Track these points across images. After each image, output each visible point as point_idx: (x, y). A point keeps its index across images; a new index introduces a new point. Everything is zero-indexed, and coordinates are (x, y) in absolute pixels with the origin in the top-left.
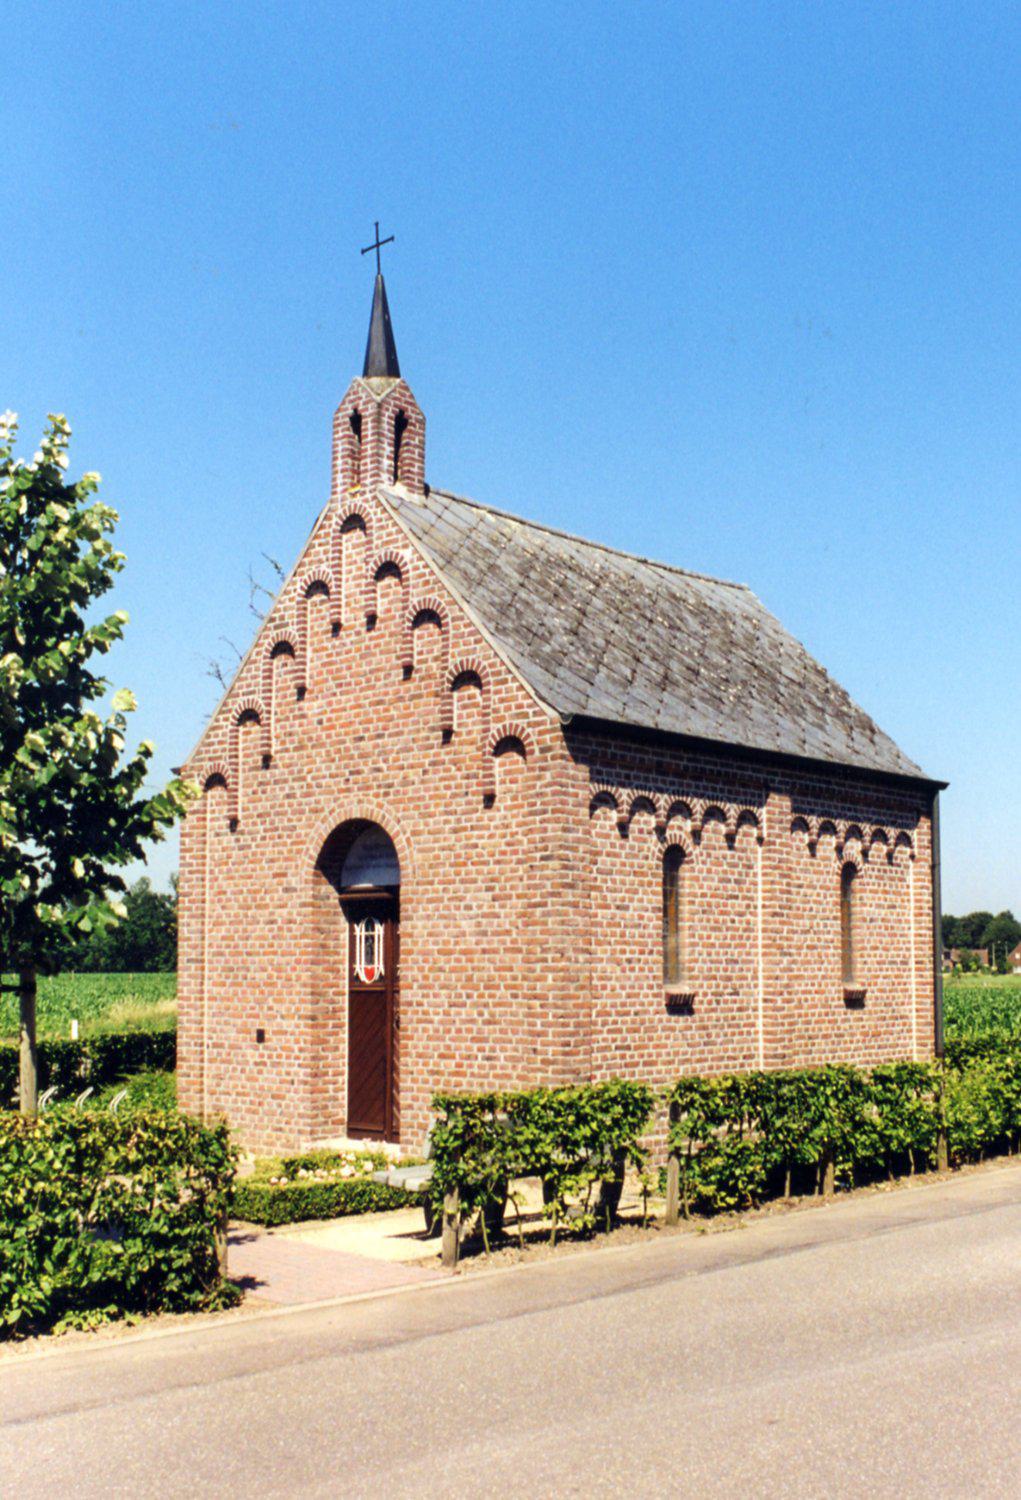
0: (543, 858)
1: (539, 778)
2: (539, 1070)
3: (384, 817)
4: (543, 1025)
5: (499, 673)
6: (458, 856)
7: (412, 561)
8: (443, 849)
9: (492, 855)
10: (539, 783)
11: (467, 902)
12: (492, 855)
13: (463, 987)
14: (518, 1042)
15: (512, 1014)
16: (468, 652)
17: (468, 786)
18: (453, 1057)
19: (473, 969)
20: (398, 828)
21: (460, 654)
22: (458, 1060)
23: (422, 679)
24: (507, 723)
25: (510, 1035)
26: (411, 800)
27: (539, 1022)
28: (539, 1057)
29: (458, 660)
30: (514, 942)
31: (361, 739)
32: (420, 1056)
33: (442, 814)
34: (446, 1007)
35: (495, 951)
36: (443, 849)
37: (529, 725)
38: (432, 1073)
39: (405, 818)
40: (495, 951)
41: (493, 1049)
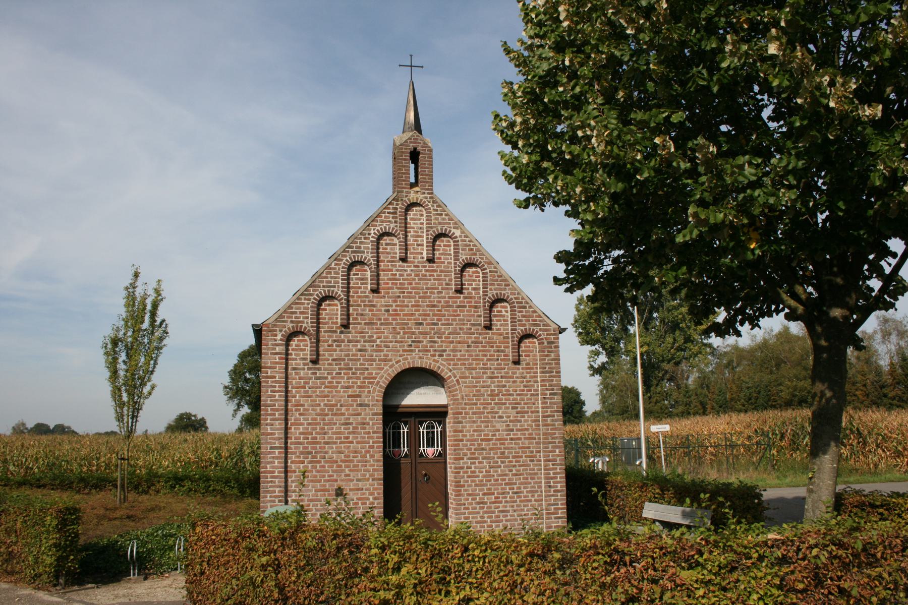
0: (551, 394)
1: (547, 356)
2: (553, 495)
3: (439, 367)
4: (554, 474)
5: (521, 303)
6: (493, 391)
7: (460, 236)
8: (483, 387)
9: (516, 391)
10: (547, 358)
11: (500, 414)
12: (516, 391)
13: (498, 458)
14: (534, 483)
15: (530, 470)
16: (501, 289)
17: (498, 356)
18: (493, 494)
19: (505, 448)
20: (450, 374)
21: (495, 290)
22: (496, 495)
23: (465, 298)
24: (528, 327)
25: (529, 480)
26: (459, 360)
27: (551, 472)
28: (552, 489)
29: (495, 292)
30: (531, 434)
31: (421, 324)
32: (469, 495)
33: (481, 369)
34: (488, 468)
35: (519, 439)
36: (483, 387)
37: (541, 330)
38: (479, 503)
39: (454, 369)
40: (519, 439)
41: (520, 488)
